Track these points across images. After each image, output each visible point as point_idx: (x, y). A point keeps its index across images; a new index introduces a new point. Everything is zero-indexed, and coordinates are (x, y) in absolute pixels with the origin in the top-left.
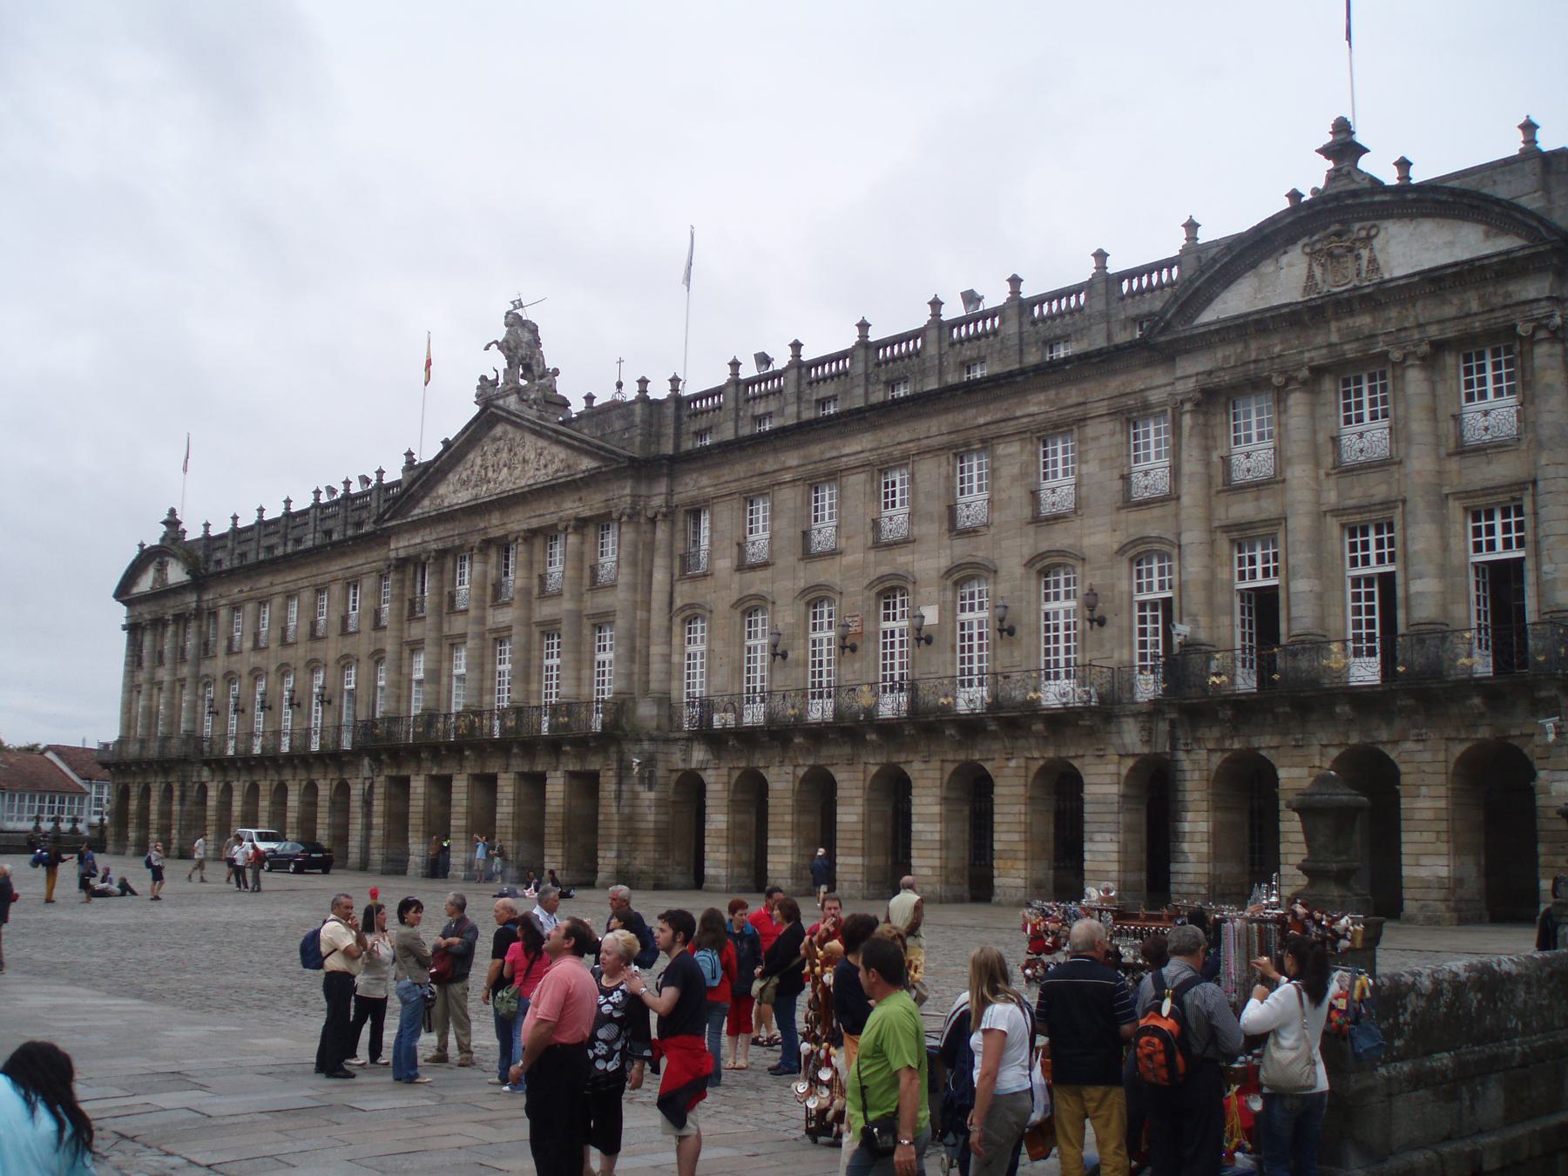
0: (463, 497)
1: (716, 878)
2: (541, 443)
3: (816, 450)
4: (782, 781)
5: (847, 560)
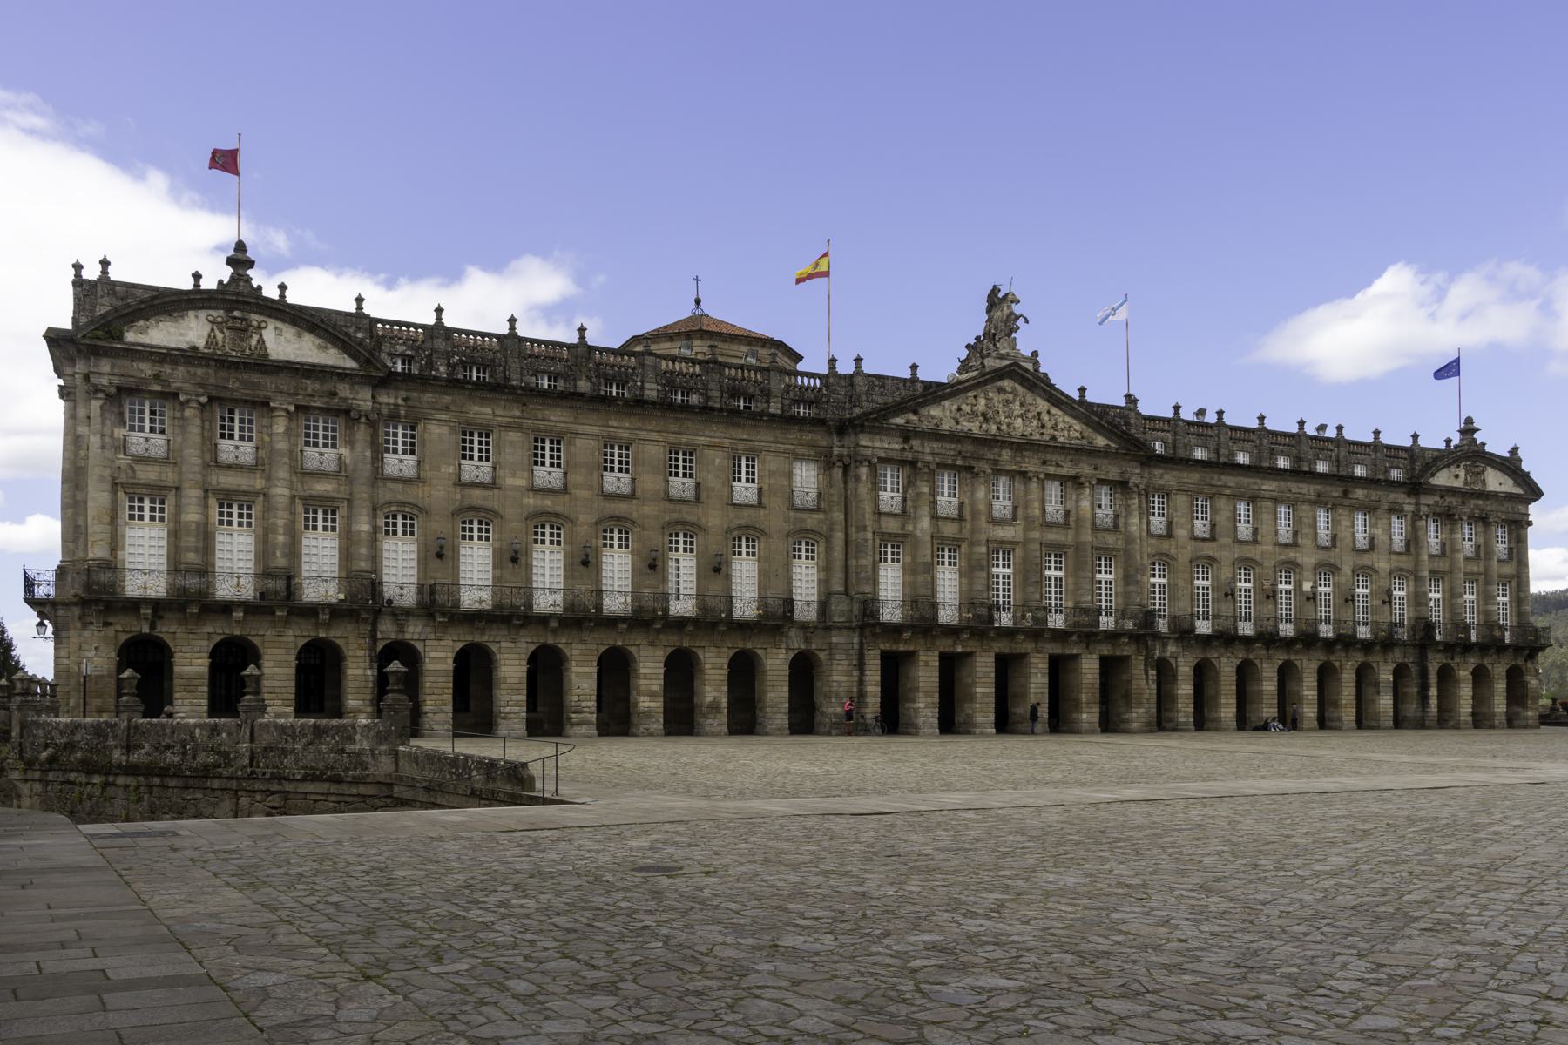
0: (974, 427)
1: (1186, 723)
2: (1054, 410)
3: (1245, 481)
4: (1227, 666)
5: (1260, 548)
